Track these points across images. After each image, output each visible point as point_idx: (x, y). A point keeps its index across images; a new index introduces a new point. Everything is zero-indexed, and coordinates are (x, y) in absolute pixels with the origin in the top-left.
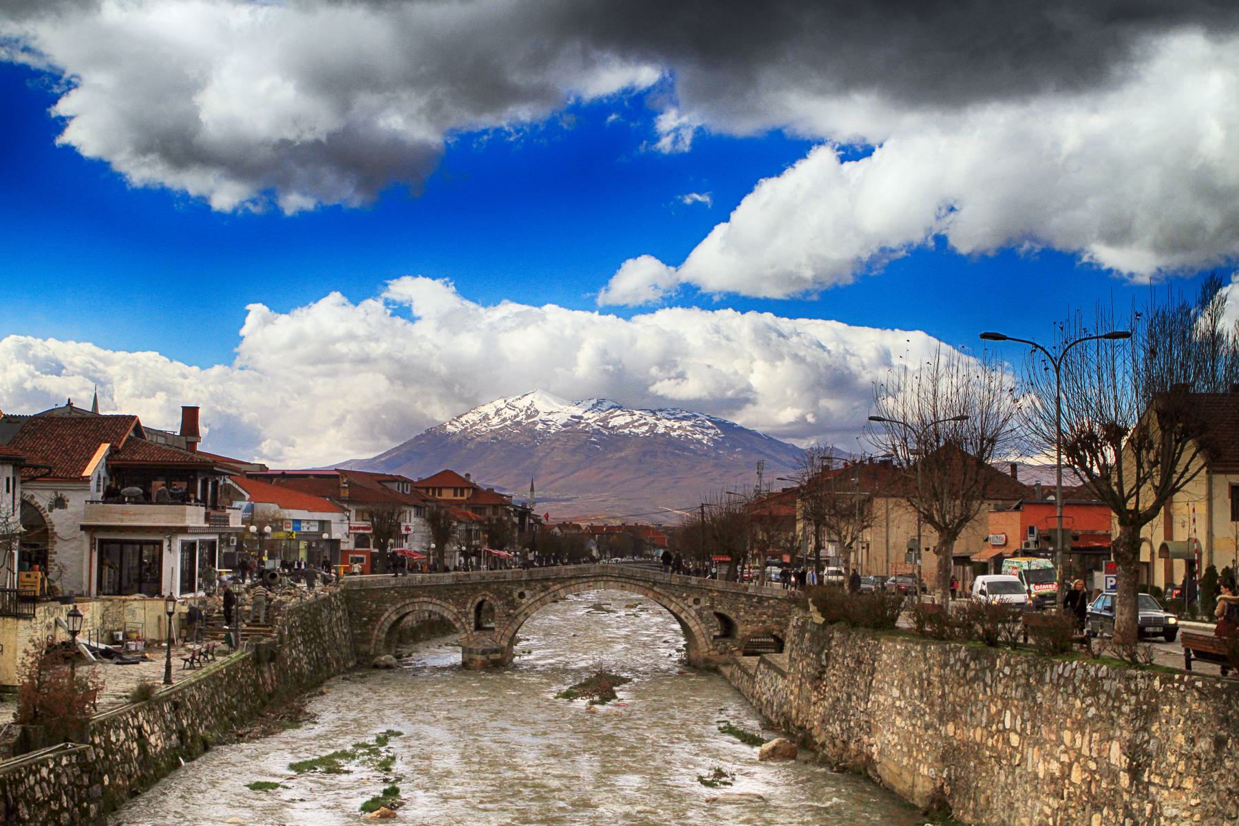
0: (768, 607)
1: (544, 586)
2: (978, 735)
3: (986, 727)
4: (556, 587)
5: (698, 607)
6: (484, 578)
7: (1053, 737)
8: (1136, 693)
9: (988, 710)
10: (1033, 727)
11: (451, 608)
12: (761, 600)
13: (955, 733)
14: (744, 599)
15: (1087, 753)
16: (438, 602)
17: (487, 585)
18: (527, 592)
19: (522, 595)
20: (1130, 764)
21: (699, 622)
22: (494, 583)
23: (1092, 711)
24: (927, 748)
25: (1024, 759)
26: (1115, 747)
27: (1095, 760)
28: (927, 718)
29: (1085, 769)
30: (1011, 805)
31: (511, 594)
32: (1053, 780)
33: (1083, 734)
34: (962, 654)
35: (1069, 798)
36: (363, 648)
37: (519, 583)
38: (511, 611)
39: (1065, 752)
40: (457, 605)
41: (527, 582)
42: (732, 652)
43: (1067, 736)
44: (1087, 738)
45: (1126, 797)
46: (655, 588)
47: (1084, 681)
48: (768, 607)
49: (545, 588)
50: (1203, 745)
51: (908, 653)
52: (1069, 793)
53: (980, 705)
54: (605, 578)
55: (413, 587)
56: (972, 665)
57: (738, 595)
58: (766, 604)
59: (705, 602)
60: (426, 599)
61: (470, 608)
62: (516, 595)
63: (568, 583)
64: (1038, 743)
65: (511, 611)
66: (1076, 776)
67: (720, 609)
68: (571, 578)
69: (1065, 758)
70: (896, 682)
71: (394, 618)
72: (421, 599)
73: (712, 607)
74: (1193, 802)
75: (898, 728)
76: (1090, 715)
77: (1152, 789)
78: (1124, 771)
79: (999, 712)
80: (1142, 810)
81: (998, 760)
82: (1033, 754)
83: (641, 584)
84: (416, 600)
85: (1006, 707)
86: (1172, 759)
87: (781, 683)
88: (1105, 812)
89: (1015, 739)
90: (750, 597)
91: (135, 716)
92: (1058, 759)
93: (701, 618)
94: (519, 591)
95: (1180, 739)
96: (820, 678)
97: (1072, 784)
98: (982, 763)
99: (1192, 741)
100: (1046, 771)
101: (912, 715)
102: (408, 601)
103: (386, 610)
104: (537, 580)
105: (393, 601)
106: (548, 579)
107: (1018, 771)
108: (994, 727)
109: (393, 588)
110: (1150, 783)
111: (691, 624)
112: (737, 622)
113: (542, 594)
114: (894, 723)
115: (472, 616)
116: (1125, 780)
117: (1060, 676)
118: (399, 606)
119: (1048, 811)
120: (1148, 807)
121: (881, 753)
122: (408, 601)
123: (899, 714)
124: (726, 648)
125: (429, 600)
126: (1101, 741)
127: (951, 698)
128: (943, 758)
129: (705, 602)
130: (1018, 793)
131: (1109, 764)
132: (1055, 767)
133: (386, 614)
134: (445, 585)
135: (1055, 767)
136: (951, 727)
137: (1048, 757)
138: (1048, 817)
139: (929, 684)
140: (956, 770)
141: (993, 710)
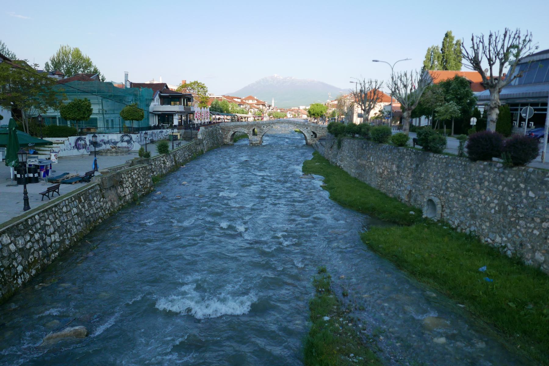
2: (364, 162)
17: (255, 125)
18: (265, 127)
23: (390, 157)
25: (374, 168)
26: (394, 166)
27: (390, 169)
29: (388, 171)
30: (371, 179)
34: (362, 143)
36: (225, 140)
40: (248, 129)
43: (384, 163)
45: (396, 178)
47: (389, 150)
50: (414, 166)
51: (350, 142)
56: (364, 145)
57: (317, 127)
59: (309, 129)
61: (251, 130)
62: (262, 127)
64: (378, 165)
66: (386, 173)
67: (313, 130)
71: (233, 133)
74: (410, 180)
77: (402, 176)
79: (370, 157)
80: (399, 181)
81: (369, 168)
82: (376, 167)
85: (371, 156)
86: (407, 169)
87: (324, 149)
89: (373, 164)
91: (163, 158)
95: (409, 164)
96: (331, 148)
99: (411, 165)
101: (351, 157)
105: (232, 129)
107: (373, 171)
111: (306, 134)
114: (347, 159)
115: (252, 133)
116: (396, 174)
119: (379, 181)
120: (401, 181)
121: (344, 166)
127: (359, 153)
128: (357, 168)
130: (373, 177)
132: (381, 170)
135: (381, 170)
136: (359, 160)
137: (379, 168)
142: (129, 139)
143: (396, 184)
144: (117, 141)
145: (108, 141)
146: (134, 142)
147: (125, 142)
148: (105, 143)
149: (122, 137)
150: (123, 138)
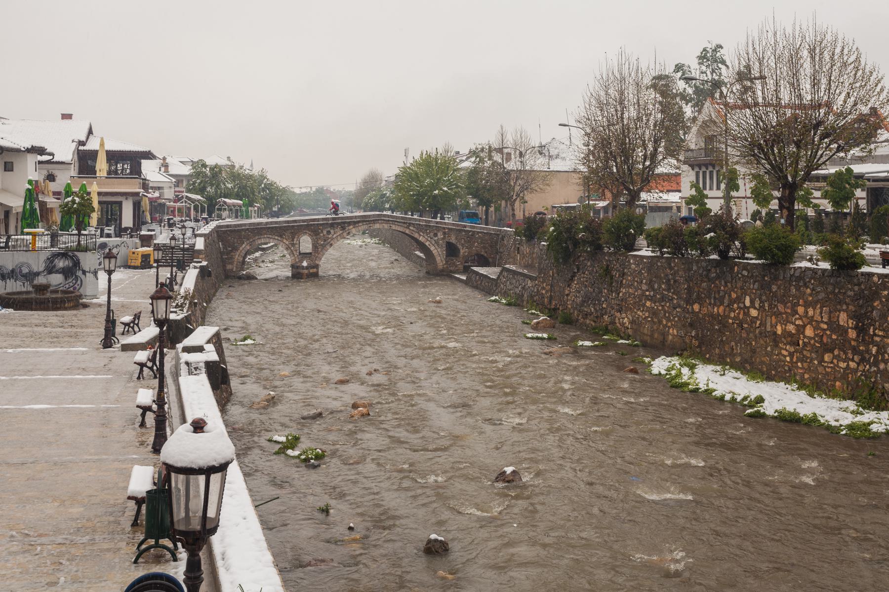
1: (342, 227)
3: (728, 306)
5: (436, 238)
7: (789, 311)
8: (859, 284)
9: (730, 296)
10: (770, 305)
13: (700, 310)
15: (819, 319)
18: (332, 231)
19: (329, 232)
20: (857, 324)
24: (676, 319)
28: (675, 302)
31: (322, 232)
32: (790, 334)
33: (814, 309)
35: (805, 344)
39: (799, 319)
43: (801, 310)
44: (818, 311)
45: (853, 343)
52: (804, 342)
53: (722, 294)
64: (778, 314)
66: (809, 332)
69: (799, 322)
70: (644, 281)
75: (647, 307)
76: (820, 297)
78: (852, 328)
87: (529, 283)
88: (836, 352)
92: (794, 324)
93: (438, 245)
97: (805, 337)
98: (724, 326)
100: (784, 331)
101: (663, 299)
108: (735, 306)
110: (875, 335)
111: (432, 248)
112: (460, 247)
114: (644, 305)
116: (852, 334)
117: (791, 276)
119: (784, 353)
123: (649, 300)
126: (830, 312)
131: (839, 325)
132: (791, 328)
136: (696, 307)
138: (785, 356)
139: (675, 281)
140: (703, 331)
141: (734, 295)
143: (856, 358)
144: (35, 270)
146: (84, 272)
147: (57, 272)
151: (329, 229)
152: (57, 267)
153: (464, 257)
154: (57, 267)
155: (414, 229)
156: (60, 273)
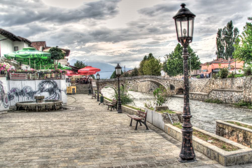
0: (181, 83)
1: (134, 80)
4: (137, 80)
5: (167, 83)
6: (121, 79)
11: (114, 86)
12: (179, 81)
14: (176, 81)
16: (111, 85)
18: (131, 82)
21: (167, 86)
22: (124, 80)
37: (129, 80)
38: (128, 86)
41: (131, 80)
42: (174, 93)
46: (158, 80)
48: (181, 83)
49: (135, 81)
54: (147, 78)
55: (106, 82)
57: (175, 80)
58: (180, 82)
60: (109, 84)
62: (128, 82)
63: (139, 79)
65: (128, 86)
67: (171, 84)
68: (140, 78)
72: (108, 84)
73: (170, 83)
83: (155, 79)
84: (106, 85)
90: (177, 81)
93: (167, 86)
94: (129, 81)
102: (105, 85)
103: (100, 87)
104: (133, 79)
106: (135, 79)
109: (101, 82)
111: (165, 87)
112: (175, 86)
113: (134, 82)
118: (103, 86)
122: (105, 85)
124: (173, 92)
125: (109, 84)
129: (168, 82)
133: (100, 88)
134: (113, 81)
142: (52, 87)
145: (22, 91)
147: (45, 91)
148: (17, 94)
149: (41, 84)
150: (42, 86)
151: (130, 81)
152: (45, 89)
153: (177, 89)
154: (45, 89)
155: (159, 80)
156: (47, 91)
